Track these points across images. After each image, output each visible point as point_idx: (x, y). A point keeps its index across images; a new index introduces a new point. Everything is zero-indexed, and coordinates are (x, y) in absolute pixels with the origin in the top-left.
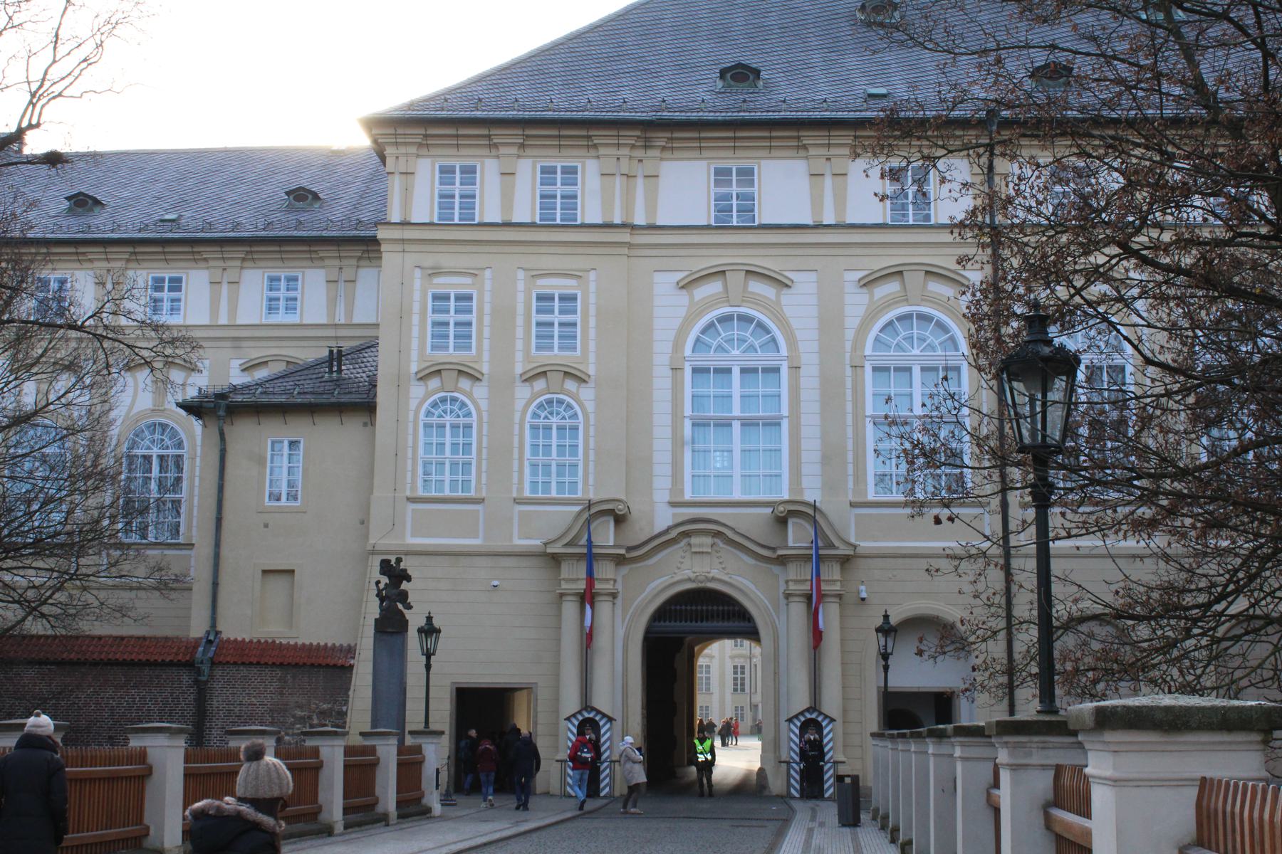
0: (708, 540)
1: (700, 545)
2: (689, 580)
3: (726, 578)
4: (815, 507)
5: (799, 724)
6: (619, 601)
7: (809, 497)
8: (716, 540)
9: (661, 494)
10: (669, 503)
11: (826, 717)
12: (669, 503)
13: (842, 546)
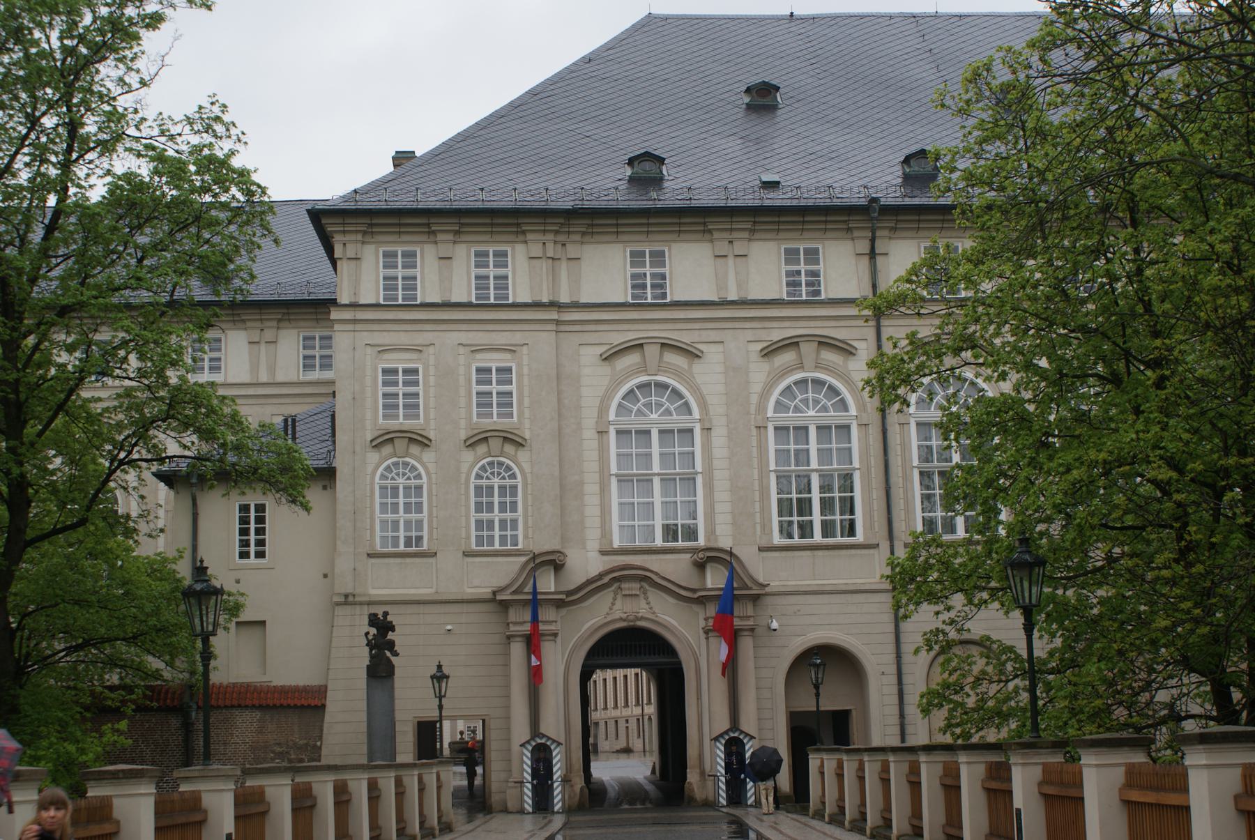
0: (637, 585)
1: (631, 589)
2: (621, 619)
4: (731, 553)
7: (725, 543)
9: (593, 545)
11: (747, 735)
13: (754, 587)
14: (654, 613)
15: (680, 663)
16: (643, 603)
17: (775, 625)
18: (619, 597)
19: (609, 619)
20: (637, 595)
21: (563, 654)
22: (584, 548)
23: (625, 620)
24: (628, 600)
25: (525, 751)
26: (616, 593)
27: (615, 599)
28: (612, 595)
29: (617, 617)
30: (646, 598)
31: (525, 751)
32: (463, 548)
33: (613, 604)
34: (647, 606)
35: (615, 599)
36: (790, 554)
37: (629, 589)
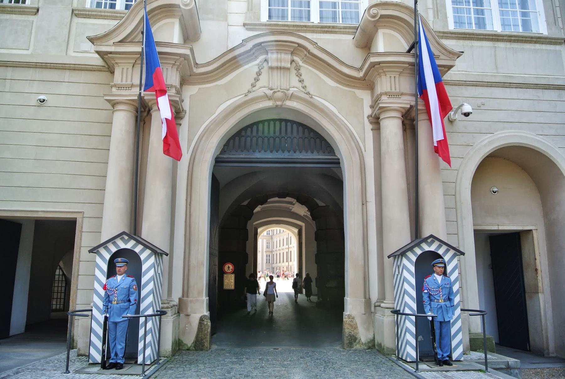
3: (307, 97)
5: (414, 258)
8: (295, 58)
13: (442, 57)
14: (308, 93)
15: (337, 162)
16: (295, 81)
17: (467, 108)
19: (250, 96)
20: (288, 69)
22: (226, 20)
23: (269, 98)
24: (276, 73)
25: (99, 260)
30: (299, 75)
31: (99, 260)
32: (75, 5)
33: (257, 80)
34: (299, 85)
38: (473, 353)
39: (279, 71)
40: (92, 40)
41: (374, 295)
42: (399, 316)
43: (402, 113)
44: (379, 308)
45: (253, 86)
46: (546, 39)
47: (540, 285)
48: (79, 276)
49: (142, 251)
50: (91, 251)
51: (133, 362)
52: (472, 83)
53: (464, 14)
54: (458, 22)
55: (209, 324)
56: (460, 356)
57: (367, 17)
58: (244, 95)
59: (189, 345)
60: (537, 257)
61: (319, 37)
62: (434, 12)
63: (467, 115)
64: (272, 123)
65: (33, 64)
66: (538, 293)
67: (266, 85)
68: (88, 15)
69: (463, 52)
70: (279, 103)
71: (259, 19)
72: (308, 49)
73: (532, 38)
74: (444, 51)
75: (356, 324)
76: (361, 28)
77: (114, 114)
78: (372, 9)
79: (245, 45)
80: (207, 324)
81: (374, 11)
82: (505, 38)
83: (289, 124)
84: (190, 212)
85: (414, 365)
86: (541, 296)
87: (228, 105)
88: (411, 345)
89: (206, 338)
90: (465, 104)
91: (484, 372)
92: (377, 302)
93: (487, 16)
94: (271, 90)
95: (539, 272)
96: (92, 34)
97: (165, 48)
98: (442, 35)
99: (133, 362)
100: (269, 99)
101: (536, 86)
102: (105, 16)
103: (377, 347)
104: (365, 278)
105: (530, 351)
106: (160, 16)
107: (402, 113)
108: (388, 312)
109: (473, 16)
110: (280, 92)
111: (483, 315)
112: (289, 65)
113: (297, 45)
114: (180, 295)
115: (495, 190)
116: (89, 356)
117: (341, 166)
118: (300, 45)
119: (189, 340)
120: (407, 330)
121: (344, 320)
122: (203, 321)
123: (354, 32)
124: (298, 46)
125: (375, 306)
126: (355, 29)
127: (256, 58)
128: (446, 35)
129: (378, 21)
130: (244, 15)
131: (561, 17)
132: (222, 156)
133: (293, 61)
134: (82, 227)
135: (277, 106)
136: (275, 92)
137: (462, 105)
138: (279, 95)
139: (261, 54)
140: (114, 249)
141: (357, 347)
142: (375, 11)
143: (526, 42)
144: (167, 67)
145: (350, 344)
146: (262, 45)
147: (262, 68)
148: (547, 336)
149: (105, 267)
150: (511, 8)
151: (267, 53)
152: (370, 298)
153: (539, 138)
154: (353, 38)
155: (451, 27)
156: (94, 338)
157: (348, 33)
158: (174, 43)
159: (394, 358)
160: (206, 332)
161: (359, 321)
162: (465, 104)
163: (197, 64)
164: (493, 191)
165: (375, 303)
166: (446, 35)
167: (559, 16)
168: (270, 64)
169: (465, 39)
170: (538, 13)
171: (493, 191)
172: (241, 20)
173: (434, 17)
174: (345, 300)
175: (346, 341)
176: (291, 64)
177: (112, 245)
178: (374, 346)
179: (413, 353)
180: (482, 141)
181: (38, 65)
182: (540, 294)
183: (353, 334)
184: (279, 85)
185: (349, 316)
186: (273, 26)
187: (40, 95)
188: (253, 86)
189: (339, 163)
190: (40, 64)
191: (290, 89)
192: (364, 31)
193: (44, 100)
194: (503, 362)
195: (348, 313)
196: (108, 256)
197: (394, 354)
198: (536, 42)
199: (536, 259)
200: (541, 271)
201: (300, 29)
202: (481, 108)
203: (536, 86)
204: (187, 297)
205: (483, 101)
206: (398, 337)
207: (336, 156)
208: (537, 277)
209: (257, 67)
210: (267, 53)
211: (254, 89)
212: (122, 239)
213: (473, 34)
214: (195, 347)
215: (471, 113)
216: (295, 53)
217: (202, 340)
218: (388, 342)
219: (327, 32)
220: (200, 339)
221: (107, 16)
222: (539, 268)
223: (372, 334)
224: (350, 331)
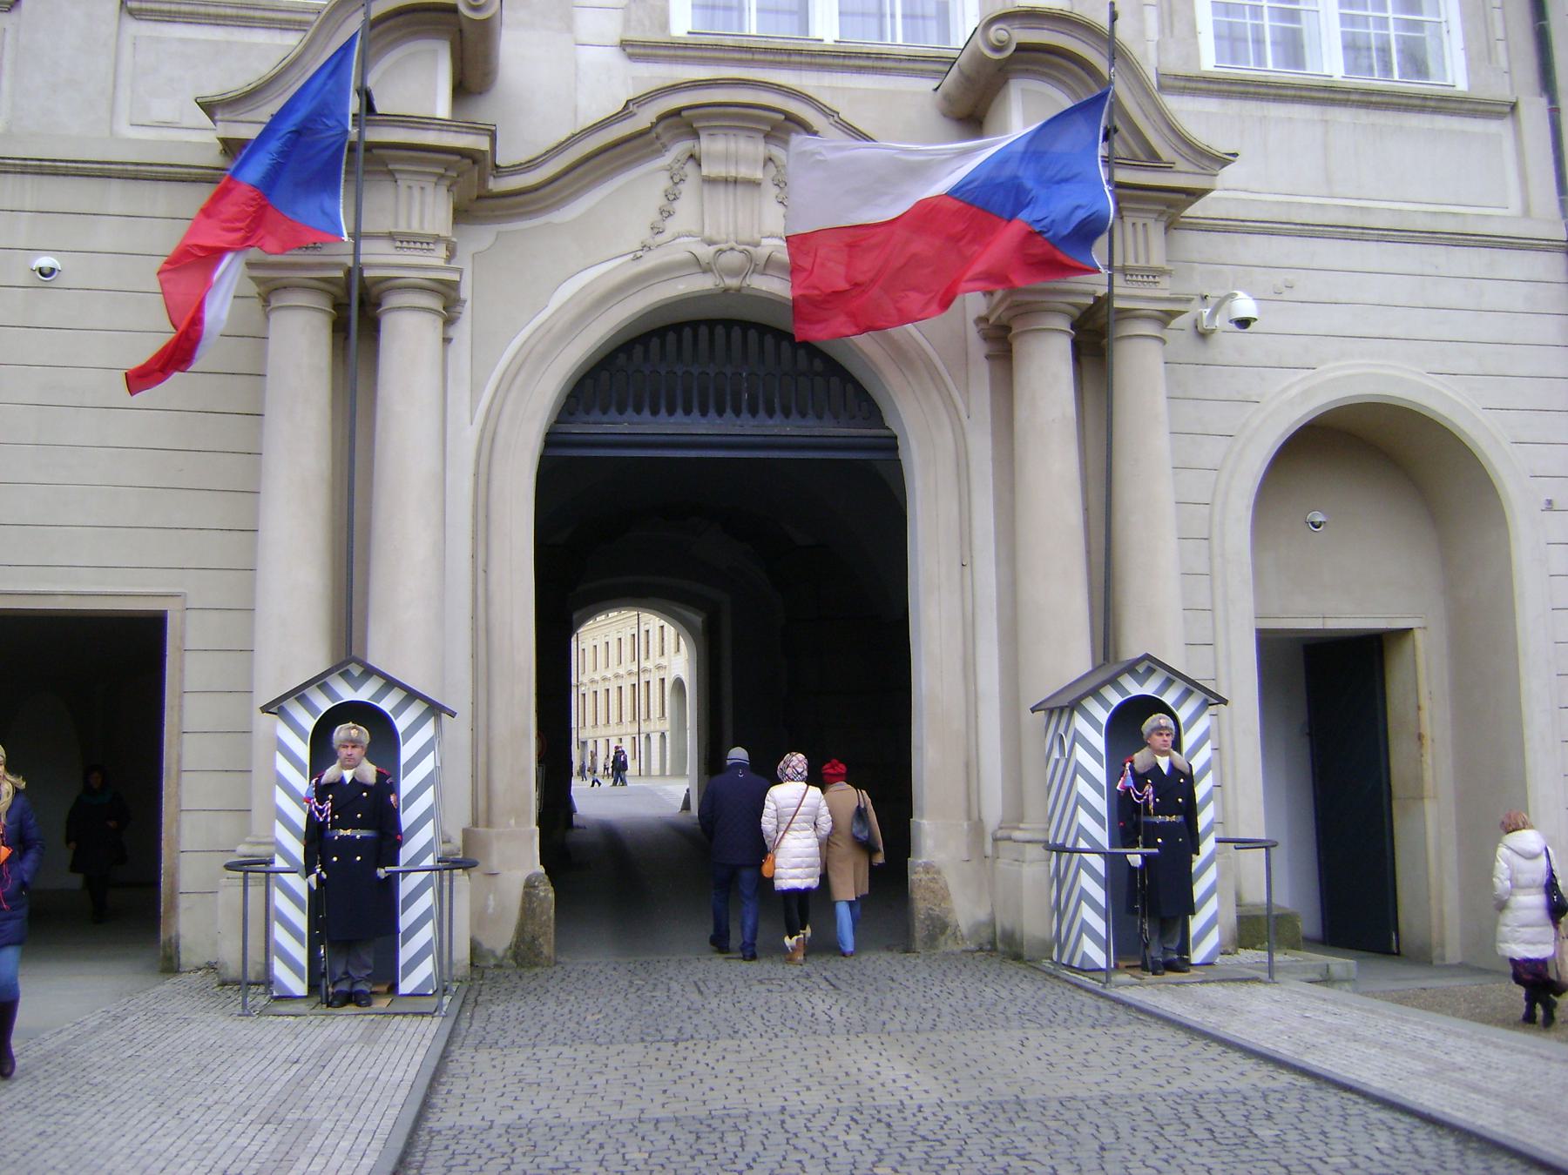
0: (756, 148)
1: (727, 158)
2: (699, 265)
5: (1103, 716)
6: (462, 331)
10: (624, 45)
12: (624, 45)
13: (1181, 165)
15: (890, 445)
17: (1245, 306)
18: (688, 190)
19: (651, 261)
20: (754, 184)
21: (476, 389)
22: (570, 28)
23: (706, 269)
24: (722, 195)
26: (677, 180)
27: (672, 196)
28: (664, 182)
29: (679, 251)
33: (667, 214)
35: (672, 196)
36: (1252, 108)
37: (727, 158)
38: (1241, 951)
39: (731, 188)
40: (209, 107)
41: (993, 810)
42: (1065, 856)
43: (1072, 316)
44: (1007, 843)
45: (657, 231)
46: (1461, 101)
47: (1428, 776)
48: (184, 774)
49: (400, 709)
50: (266, 709)
51: (384, 988)
52: (1262, 225)
53: (1244, 17)
54: (1229, 40)
55: (552, 895)
56: (1212, 954)
57: (979, 49)
58: (631, 256)
59: (500, 952)
60: (1424, 702)
61: (840, 85)
62: (1161, 17)
63: (1244, 323)
64: (703, 331)
65: (17, 162)
66: (1422, 798)
67: (695, 229)
68: (170, 12)
69: (1235, 155)
70: (733, 282)
71: (665, 25)
72: (812, 127)
73: (1425, 98)
74: (1184, 150)
75: (947, 887)
76: (961, 71)
77: (271, 320)
78: (994, 28)
79: (635, 114)
80: (546, 896)
81: (997, 33)
82: (1353, 97)
83: (753, 334)
84: (487, 590)
85: (1103, 977)
86: (1429, 807)
87: (583, 283)
88: (1094, 935)
89: (545, 933)
90: (1241, 294)
91: (1266, 983)
92: (1001, 828)
93: (1306, 25)
94: (709, 245)
95: (1427, 742)
96: (212, 91)
97: (420, 131)
98: (1182, 84)
99: (384, 988)
100: (705, 272)
101: (1432, 238)
102: (217, 16)
103: (1000, 946)
104: (967, 765)
105: (1398, 954)
106: (571, 190)
107: (1072, 316)
108: (1035, 852)
109: (1267, 23)
110: (736, 253)
111: (1266, 847)
112: (758, 174)
113: (783, 117)
114: (465, 820)
115: (1319, 518)
116: (267, 980)
117: (900, 457)
118: (790, 118)
119: (501, 939)
120: (1084, 896)
121: (912, 877)
122: (535, 887)
123: (941, 72)
124: (786, 119)
125: (996, 840)
126: (945, 62)
127: (665, 147)
128: (1193, 85)
129: (1009, 60)
130: (618, 15)
131: (1506, 39)
132: (564, 428)
133: (770, 159)
134: (182, 638)
135: (726, 290)
136: (721, 251)
137: (1232, 296)
138: (733, 259)
139: (677, 138)
140: (324, 704)
141: (947, 945)
142: (1003, 35)
143: (1408, 108)
144: (423, 184)
145: (932, 939)
146: (684, 114)
147: (681, 180)
148: (1441, 912)
149: (303, 751)
150: (1373, 10)
151: (695, 134)
152: (980, 820)
153: (1434, 383)
154: (936, 89)
155: (1208, 62)
156: (280, 934)
157: (922, 74)
158: (438, 117)
159: (1047, 965)
160: (545, 917)
161: (952, 879)
162: (1241, 294)
163: (497, 167)
164: (1312, 523)
165: (996, 831)
166: (1193, 85)
167: (1500, 34)
168: (705, 171)
169: (1244, 96)
170: (1444, 24)
171: (1312, 523)
172: (612, 28)
173: (1161, 31)
174: (912, 826)
175: (920, 932)
176: (764, 166)
177: (319, 691)
178: (993, 943)
179: (1099, 957)
180: (1284, 391)
181: (31, 166)
182: (1426, 801)
183: (937, 913)
184: (731, 229)
185: (928, 868)
186: (707, 49)
187: (38, 257)
188: (656, 231)
189: (894, 448)
190: (38, 163)
191: (765, 242)
192: (968, 81)
193: (53, 270)
194: (1315, 966)
195: (924, 860)
196: (309, 723)
197: (1046, 958)
198: (1436, 111)
199: (1419, 708)
200: (1433, 740)
201: (785, 58)
202: (1286, 296)
203: (1432, 238)
204: (489, 824)
205: (1290, 276)
206: (1059, 909)
207: (888, 428)
208: (1422, 756)
209: (666, 175)
210: (695, 134)
211: (660, 239)
212: (346, 675)
213: (1267, 85)
214: (516, 960)
215: (1255, 320)
216: (775, 137)
217: (534, 939)
218: (1034, 924)
219: (860, 70)
220: (528, 938)
221: (225, 17)
222: (1427, 730)
223: (988, 910)
224: (929, 906)
